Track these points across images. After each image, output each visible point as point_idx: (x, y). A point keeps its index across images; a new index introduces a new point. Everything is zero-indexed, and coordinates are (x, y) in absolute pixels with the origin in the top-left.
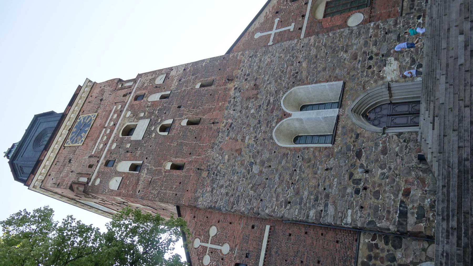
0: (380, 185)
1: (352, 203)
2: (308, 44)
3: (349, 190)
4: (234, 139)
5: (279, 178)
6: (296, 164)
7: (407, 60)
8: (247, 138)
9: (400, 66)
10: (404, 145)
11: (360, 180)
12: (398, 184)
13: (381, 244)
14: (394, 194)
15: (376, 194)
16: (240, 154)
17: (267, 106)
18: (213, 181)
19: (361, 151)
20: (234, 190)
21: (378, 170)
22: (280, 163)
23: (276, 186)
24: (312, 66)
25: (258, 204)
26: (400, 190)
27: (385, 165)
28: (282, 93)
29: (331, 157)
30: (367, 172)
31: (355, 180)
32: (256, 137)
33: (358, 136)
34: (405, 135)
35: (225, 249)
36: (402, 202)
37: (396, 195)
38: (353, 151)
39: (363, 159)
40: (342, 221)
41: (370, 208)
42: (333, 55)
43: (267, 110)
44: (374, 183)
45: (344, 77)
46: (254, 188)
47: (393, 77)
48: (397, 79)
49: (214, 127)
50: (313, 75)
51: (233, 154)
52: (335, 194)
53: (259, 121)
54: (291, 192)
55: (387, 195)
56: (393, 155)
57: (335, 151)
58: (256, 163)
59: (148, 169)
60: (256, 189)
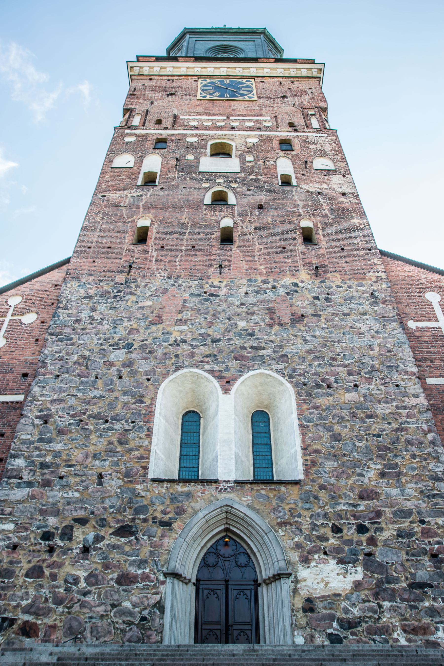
0: (54, 577)
1: (26, 529)
2: (405, 394)
3: (52, 521)
5: (95, 397)
6: (118, 420)
7: (356, 612)
8: (184, 328)
9: (339, 595)
10: (134, 617)
11: (70, 539)
12: (50, 610)
14: (31, 606)
16: (152, 323)
17: (252, 347)
18: (105, 294)
20: (83, 329)
21: (86, 570)
22: (125, 393)
23: (80, 395)
24: (345, 414)
25: (52, 374)
26: (36, 615)
27: (96, 584)
29: (126, 480)
30: (86, 550)
31: (72, 530)
32: (184, 341)
33: (167, 524)
34: (158, 620)
36: (12, 621)
38: (133, 520)
39: (114, 540)
41: (11, 563)
42: (374, 449)
43: (243, 347)
44: (60, 565)
45: (313, 481)
46: (82, 360)
47: (309, 583)
50: (321, 418)
51: (152, 312)
52: (48, 497)
53: (219, 340)
55: (32, 592)
56: (116, 597)
57: (138, 487)
59: (141, 196)
60: (79, 364)
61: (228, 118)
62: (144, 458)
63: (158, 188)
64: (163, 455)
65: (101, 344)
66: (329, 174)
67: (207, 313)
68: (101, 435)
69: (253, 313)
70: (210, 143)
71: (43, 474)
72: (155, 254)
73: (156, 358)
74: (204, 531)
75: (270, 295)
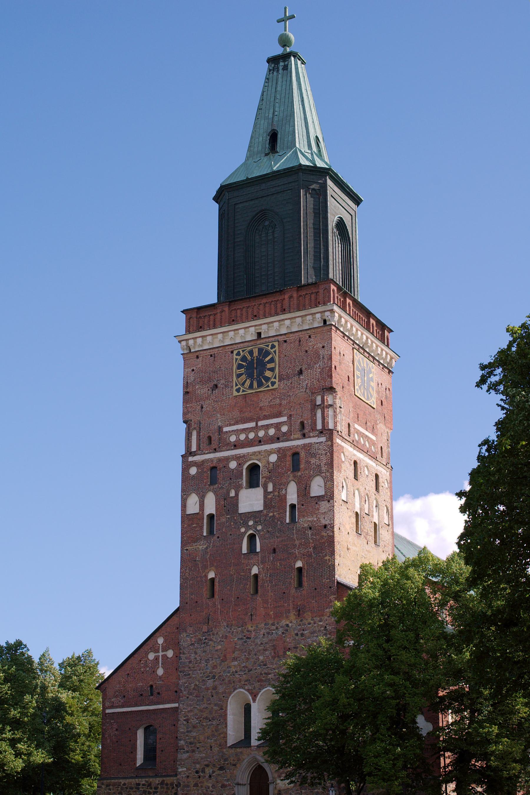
3: (198, 766)
4: (236, 648)
8: (236, 663)
11: (205, 773)
13: (174, 791)
15: (196, 785)
16: (223, 661)
17: (265, 673)
19: (224, 769)
20: (194, 667)
22: (215, 705)
30: (210, 776)
33: (235, 765)
35: (160, 672)
40: (179, 765)
43: (261, 674)
44: (203, 783)
46: (196, 687)
47: (280, 785)
48: (278, 788)
54: (194, 721)
58: (215, 681)
59: (207, 548)
61: (257, 424)
62: (225, 737)
63: (215, 537)
64: (233, 732)
65: (202, 677)
66: (319, 500)
67: (245, 652)
68: (209, 728)
70: (245, 466)
71: (191, 747)
72: (219, 607)
73: (225, 683)
75: (274, 636)
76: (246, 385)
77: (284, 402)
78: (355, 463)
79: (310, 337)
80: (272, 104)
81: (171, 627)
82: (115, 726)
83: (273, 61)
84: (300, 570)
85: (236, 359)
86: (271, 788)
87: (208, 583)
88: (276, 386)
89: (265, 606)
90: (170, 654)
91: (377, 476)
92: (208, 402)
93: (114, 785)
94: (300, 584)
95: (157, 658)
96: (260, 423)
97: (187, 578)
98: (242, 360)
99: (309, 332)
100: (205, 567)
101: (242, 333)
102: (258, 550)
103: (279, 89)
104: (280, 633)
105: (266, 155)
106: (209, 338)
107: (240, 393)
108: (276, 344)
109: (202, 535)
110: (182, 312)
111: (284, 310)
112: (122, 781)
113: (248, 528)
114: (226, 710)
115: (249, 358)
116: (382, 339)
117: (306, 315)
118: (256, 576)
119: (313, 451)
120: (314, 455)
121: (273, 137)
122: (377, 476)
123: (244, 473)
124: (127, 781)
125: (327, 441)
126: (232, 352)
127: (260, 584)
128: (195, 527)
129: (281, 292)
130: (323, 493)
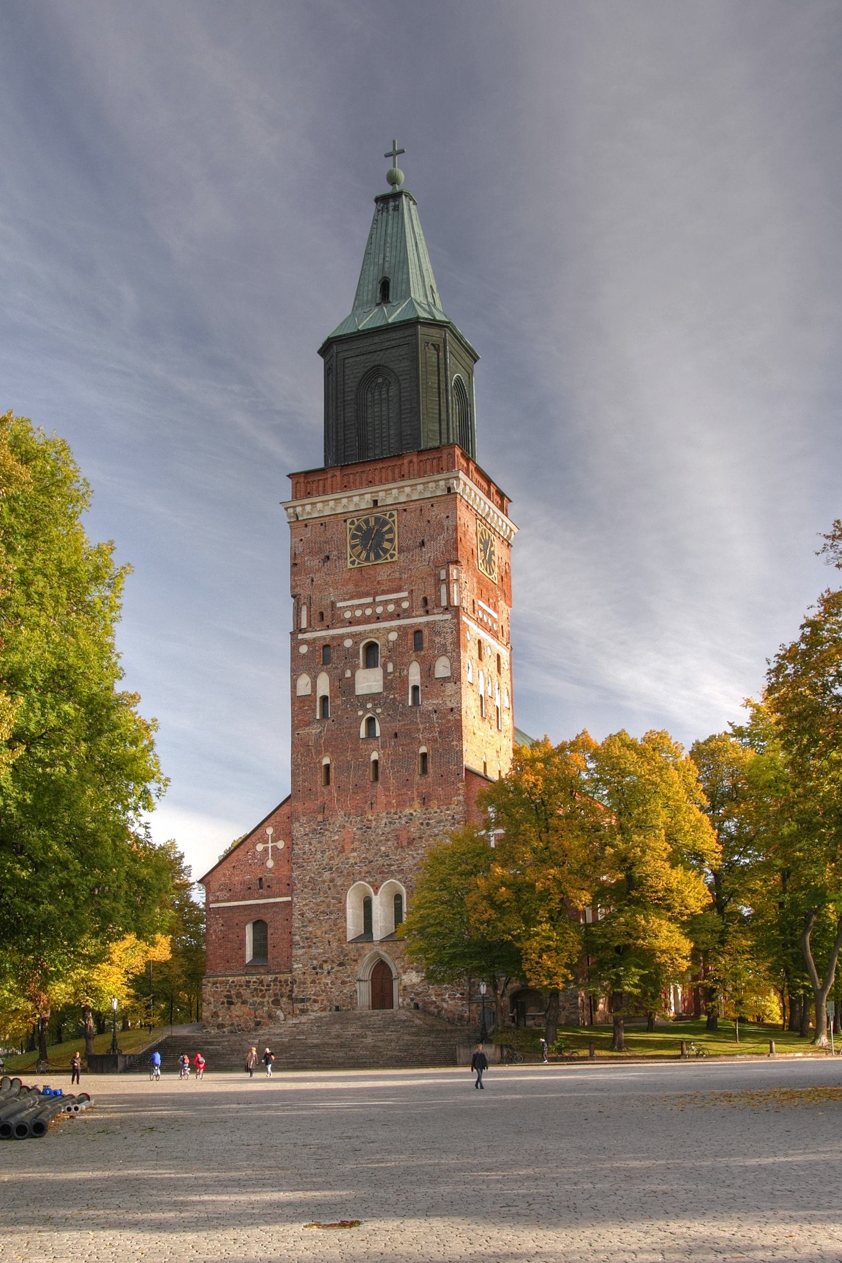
3: (315, 962)
7: (420, 990)
13: (288, 988)
15: (313, 982)
16: (340, 852)
28: (400, 877)
30: (329, 973)
33: (356, 961)
35: (270, 864)
37: (314, 995)
43: (383, 865)
44: (321, 979)
49: (367, 807)
54: (309, 915)
61: (374, 600)
62: (345, 932)
63: (330, 721)
69: (389, 840)
70: (362, 645)
74: (371, 962)
76: (361, 557)
77: (405, 576)
78: (479, 642)
79: (432, 506)
80: (382, 248)
81: (282, 817)
82: (221, 921)
83: (383, 200)
84: (424, 756)
85: (350, 529)
86: (395, 984)
87: (323, 770)
88: (395, 558)
89: (387, 793)
90: (281, 844)
91: (498, 656)
92: (318, 575)
93: (221, 982)
94: (425, 771)
95: (266, 850)
96: (378, 599)
97: (299, 765)
98: (356, 529)
99: (431, 500)
100: (319, 753)
101: (356, 501)
102: (378, 734)
103: (389, 231)
104: (403, 822)
105: (378, 305)
106: (319, 506)
107: (356, 566)
108: (395, 513)
109: (315, 719)
110: (288, 476)
111: (403, 476)
112: (231, 979)
113: (366, 711)
114: (345, 903)
115: (364, 527)
116: (502, 508)
117: (428, 482)
118: (376, 762)
119: (437, 629)
120: (439, 634)
121: (385, 286)
122: (498, 656)
123: (361, 653)
124: (236, 979)
125: (452, 619)
126: (345, 521)
127: (380, 770)
128: (307, 710)
129: (399, 456)
130: (449, 674)
